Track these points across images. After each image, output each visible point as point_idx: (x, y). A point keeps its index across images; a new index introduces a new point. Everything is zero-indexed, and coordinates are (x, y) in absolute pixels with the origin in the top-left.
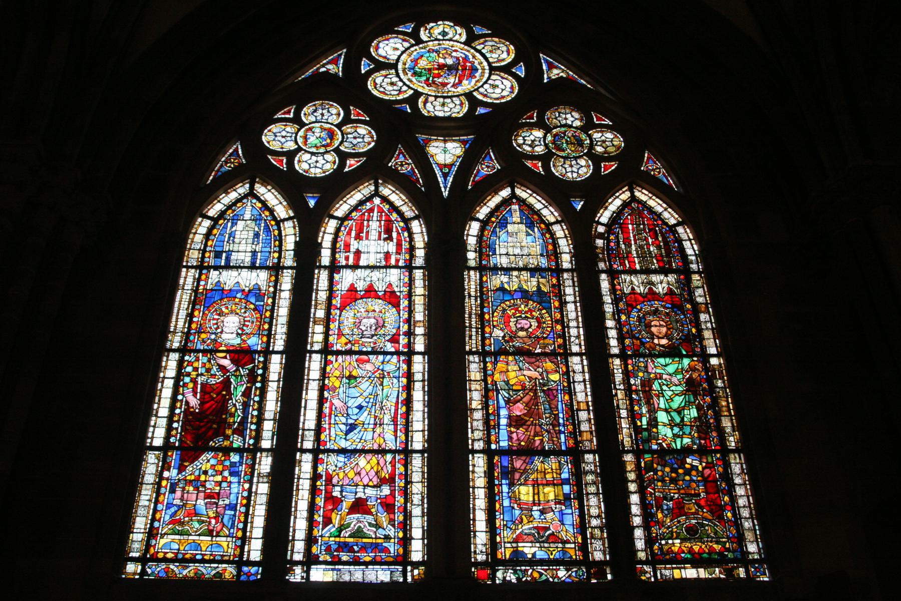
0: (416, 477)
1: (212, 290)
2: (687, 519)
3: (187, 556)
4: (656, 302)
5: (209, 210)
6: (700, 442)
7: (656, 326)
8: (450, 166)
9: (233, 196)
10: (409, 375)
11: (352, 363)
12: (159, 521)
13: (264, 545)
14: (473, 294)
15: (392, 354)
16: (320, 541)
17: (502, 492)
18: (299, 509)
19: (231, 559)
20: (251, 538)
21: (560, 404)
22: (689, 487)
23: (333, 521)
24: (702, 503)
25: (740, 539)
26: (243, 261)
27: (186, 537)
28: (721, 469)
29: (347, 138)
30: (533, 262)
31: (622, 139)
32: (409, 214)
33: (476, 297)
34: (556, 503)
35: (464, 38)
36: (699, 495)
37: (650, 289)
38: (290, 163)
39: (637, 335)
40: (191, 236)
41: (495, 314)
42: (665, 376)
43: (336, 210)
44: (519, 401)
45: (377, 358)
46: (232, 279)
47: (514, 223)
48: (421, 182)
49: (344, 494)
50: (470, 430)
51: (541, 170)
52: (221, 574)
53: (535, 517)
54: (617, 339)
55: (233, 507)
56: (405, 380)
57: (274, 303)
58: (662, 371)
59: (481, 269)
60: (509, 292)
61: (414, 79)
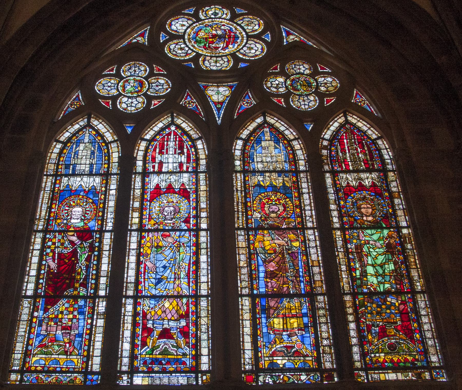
0: (203, 314)
1: (63, 190)
3: (51, 369)
4: (364, 192)
5: (61, 137)
7: (364, 208)
8: (221, 103)
9: (77, 127)
10: (197, 245)
11: (158, 237)
12: (32, 345)
13: (102, 360)
14: (239, 189)
16: (139, 357)
17: (262, 323)
18: (125, 336)
19: (80, 370)
20: (93, 356)
21: (300, 262)
23: (148, 344)
26: (84, 170)
27: (49, 356)
29: (152, 86)
30: (279, 167)
31: (338, 82)
32: (195, 136)
33: (241, 191)
34: (299, 330)
37: (360, 183)
38: (114, 104)
39: (352, 215)
40: (49, 154)
41: (255, 202)
43: (146, 135)
44: (272, 261)
45: (175, 234)
46: (77, 182)
47: (266, 140)
48: (202, 114)
49: (155, 325)
50: (239, 281)
51: (284, 104)
52: (74, 380)
53: (285, 339)
54: (338, 218)
55: (80, 335)
57: (105, 198)
58: (369, 239)
59: (245, 172)
60: (264, 187)
61: (196, 46)
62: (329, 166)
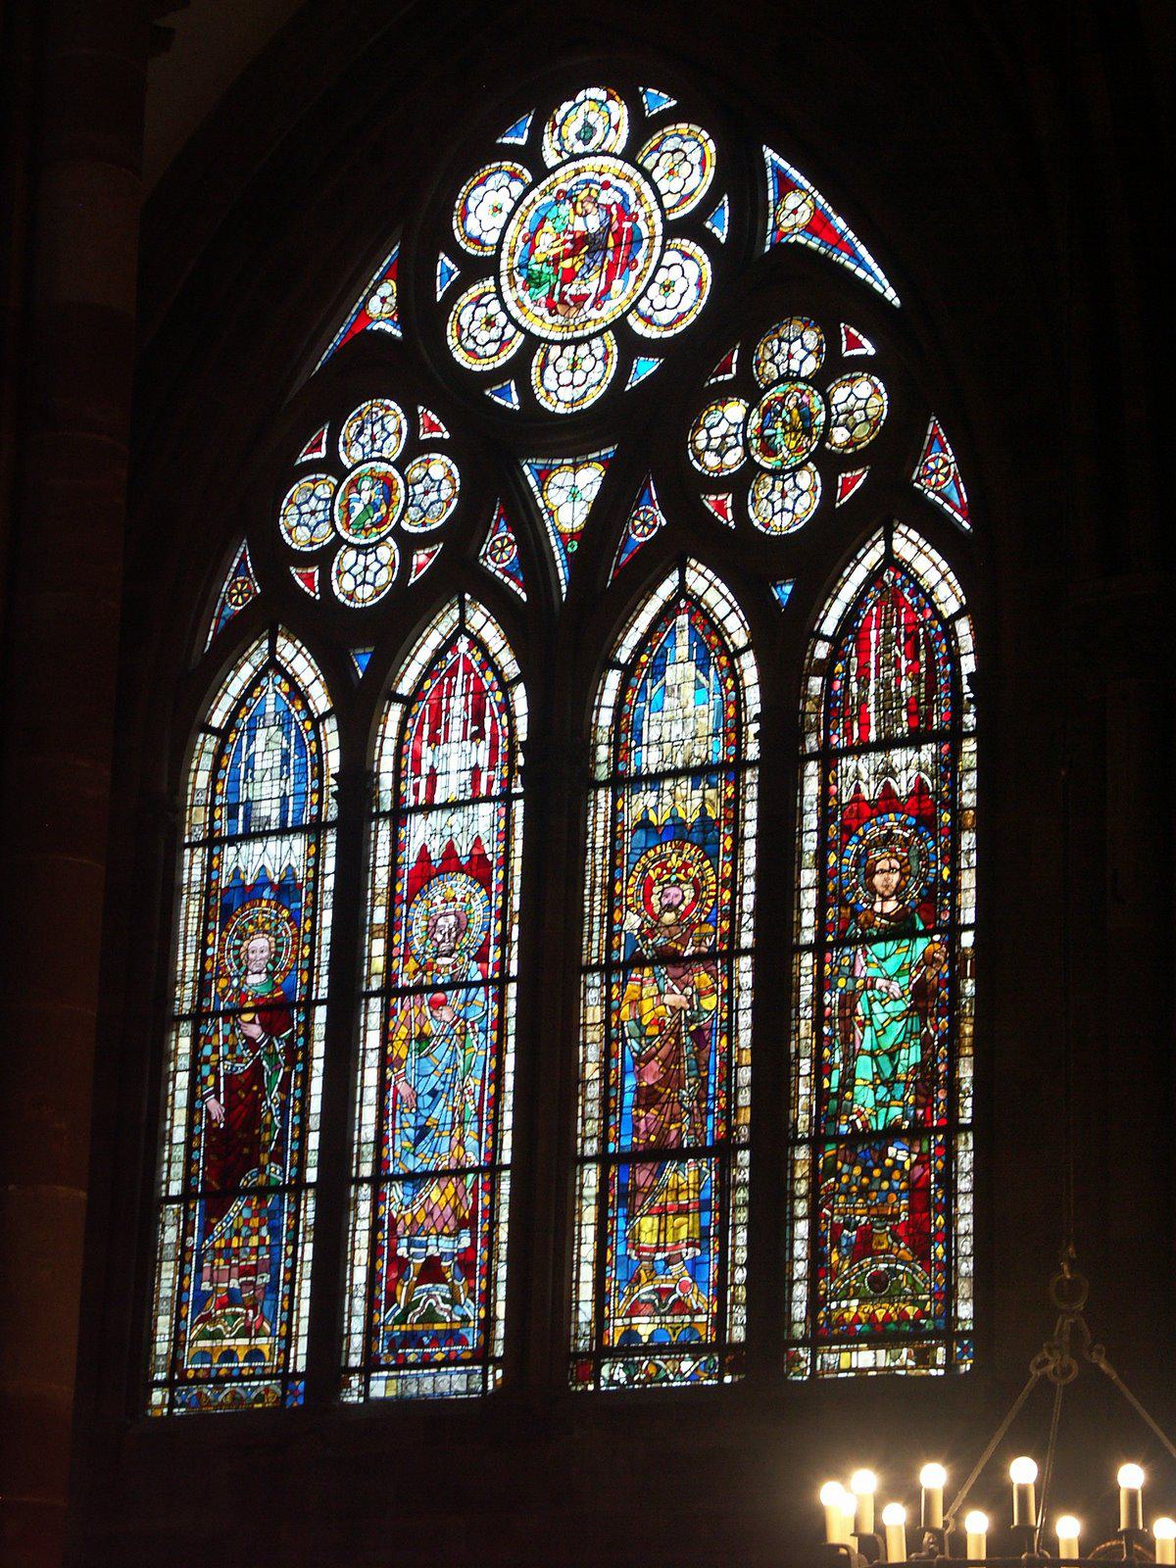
2: (872, 1262)
4: (892, 816)
6: (915, 1114)
7: (883, 871)
10: (500, 1024)
15: (477, 984)
18: (355, 1282)
22: (885, 1201)
24: (901, 1232)
25: (949, 1295)
26: (269, 818)
28: (940, 1164)
35: (619, 142)
36: (898, 1216)
42: (880, 983)
46: (256, 859)
56: (494, 1034)
62: (819, 735)
